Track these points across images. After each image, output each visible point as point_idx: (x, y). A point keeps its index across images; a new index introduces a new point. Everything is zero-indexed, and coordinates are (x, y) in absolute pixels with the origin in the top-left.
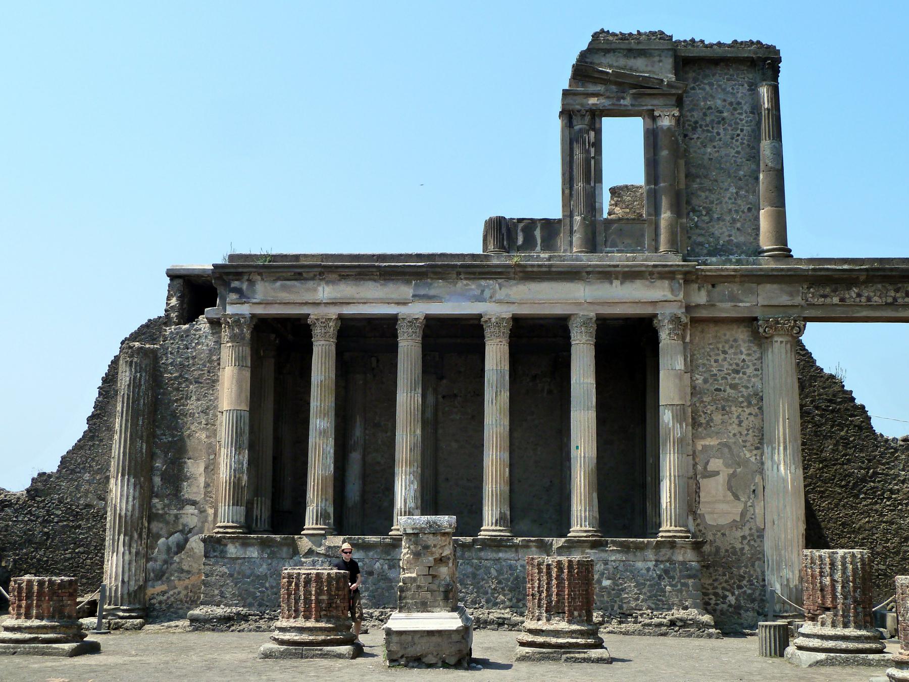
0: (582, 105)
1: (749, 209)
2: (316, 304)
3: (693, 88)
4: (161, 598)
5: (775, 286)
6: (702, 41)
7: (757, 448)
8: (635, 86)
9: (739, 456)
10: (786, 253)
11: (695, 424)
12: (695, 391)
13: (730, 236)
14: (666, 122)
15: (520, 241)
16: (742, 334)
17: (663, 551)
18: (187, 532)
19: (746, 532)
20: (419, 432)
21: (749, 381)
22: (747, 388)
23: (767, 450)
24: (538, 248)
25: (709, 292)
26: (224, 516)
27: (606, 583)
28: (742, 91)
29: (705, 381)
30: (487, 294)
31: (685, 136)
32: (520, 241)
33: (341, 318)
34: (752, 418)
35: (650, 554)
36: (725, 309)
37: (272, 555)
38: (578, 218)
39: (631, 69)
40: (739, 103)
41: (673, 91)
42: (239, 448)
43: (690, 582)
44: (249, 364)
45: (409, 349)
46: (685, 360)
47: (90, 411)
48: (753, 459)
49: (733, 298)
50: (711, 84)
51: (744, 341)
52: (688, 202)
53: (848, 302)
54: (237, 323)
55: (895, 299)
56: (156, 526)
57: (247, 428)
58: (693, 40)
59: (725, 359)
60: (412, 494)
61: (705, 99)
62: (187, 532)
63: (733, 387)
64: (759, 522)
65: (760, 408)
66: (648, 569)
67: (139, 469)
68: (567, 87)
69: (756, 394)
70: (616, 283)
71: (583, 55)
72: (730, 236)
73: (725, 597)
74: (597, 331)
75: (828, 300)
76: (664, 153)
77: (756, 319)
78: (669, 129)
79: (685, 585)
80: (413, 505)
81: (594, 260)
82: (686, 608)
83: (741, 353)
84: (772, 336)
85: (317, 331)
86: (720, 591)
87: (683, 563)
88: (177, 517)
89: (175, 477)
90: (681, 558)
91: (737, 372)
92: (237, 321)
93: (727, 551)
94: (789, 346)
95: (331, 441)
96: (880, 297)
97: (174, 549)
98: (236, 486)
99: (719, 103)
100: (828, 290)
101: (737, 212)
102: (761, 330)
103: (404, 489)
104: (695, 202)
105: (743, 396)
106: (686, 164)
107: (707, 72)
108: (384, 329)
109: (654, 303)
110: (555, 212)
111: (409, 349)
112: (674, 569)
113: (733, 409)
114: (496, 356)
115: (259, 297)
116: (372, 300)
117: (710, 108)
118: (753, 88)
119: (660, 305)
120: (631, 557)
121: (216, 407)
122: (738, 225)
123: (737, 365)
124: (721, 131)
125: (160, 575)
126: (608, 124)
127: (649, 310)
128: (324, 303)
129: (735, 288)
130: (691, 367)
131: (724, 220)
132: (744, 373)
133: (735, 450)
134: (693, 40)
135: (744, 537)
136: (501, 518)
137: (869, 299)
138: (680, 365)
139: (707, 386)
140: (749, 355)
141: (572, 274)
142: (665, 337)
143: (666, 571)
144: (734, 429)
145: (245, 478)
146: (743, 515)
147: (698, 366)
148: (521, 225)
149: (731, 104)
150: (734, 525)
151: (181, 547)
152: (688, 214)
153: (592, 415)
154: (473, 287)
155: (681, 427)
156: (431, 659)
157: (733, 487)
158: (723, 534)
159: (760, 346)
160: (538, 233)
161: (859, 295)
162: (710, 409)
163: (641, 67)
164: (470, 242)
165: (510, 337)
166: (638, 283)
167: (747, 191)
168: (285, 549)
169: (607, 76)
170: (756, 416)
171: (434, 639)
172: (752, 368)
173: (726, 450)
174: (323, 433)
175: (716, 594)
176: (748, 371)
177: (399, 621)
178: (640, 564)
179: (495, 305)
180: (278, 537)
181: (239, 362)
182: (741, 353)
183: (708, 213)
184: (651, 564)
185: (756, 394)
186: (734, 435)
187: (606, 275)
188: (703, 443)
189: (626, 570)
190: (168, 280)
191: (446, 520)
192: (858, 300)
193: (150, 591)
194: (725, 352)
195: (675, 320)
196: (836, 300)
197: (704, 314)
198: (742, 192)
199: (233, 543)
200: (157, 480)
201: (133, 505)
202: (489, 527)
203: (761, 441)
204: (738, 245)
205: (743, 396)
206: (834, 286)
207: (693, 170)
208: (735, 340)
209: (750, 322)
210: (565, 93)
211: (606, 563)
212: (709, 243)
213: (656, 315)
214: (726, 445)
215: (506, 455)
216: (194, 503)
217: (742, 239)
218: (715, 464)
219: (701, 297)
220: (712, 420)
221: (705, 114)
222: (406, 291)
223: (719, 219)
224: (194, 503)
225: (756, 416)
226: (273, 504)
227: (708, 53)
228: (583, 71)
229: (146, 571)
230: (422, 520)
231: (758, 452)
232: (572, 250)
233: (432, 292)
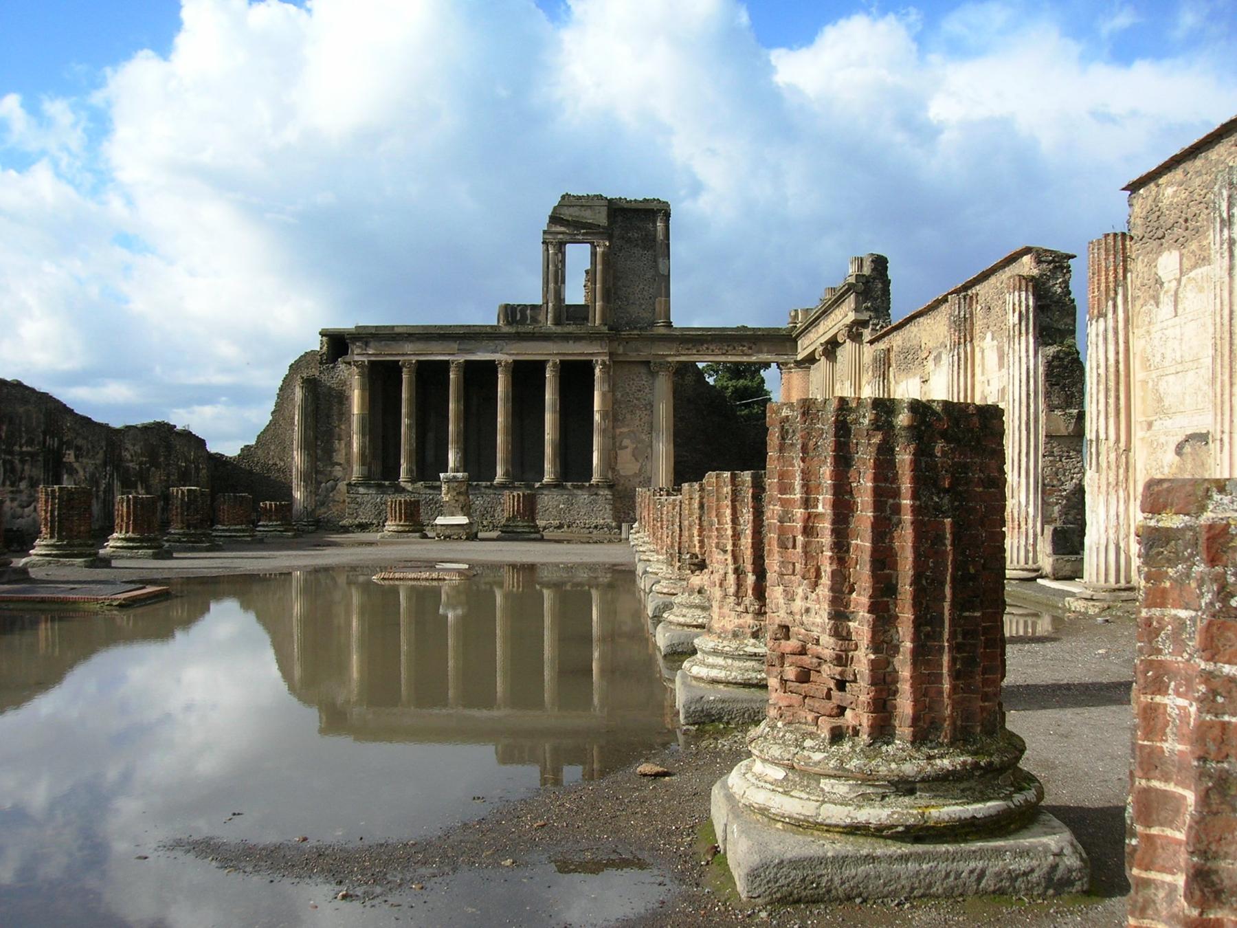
10: (669, 325)
12: (615, 402)
16: (643, 370)
18: (336, 480)
26: (356, 471)
33: (418, 361)
36: (633, 356)
38: (550, 305)
42: (363, 435)
47: (273, 408)
49: (637, 350)
56: (320, 477)
62: (336, 480)
67: (309, 446)
71: (555, 208)
81: (559, 329)
88: (331, 472)
89: (329, 452)
103: (452, 458)
109: (591, 354)
110: (539, 301)
116: (437, 353)
125: (323, 504)
126: (570, 248)
127: (589, 358)
128: (410, 354)
130: (613, 388)
141: (547, 337)
144: (637, 423)
146: (640, 470)
150: (635, 475)
151: (333, 488)
163: (588, 216)
164: (488, 317)
169: (569, 221)
174: (409, 427)
177: (440, 520)
180: (387, 483)
181: (363, 389)
187: (566, 338)
191: (460, 475)
193: (318, 512)
197: (621, 359)
200: (319, 452)
202: (499, 477)
210: (545, 232)
216: (340, 464)
217: (645, 315)
218: (626, 442)
222: (455, 346)
224: (340, 464)
226: (382, 465)
227: (626, 206)
228: (555, 219)
232: (548, 323)
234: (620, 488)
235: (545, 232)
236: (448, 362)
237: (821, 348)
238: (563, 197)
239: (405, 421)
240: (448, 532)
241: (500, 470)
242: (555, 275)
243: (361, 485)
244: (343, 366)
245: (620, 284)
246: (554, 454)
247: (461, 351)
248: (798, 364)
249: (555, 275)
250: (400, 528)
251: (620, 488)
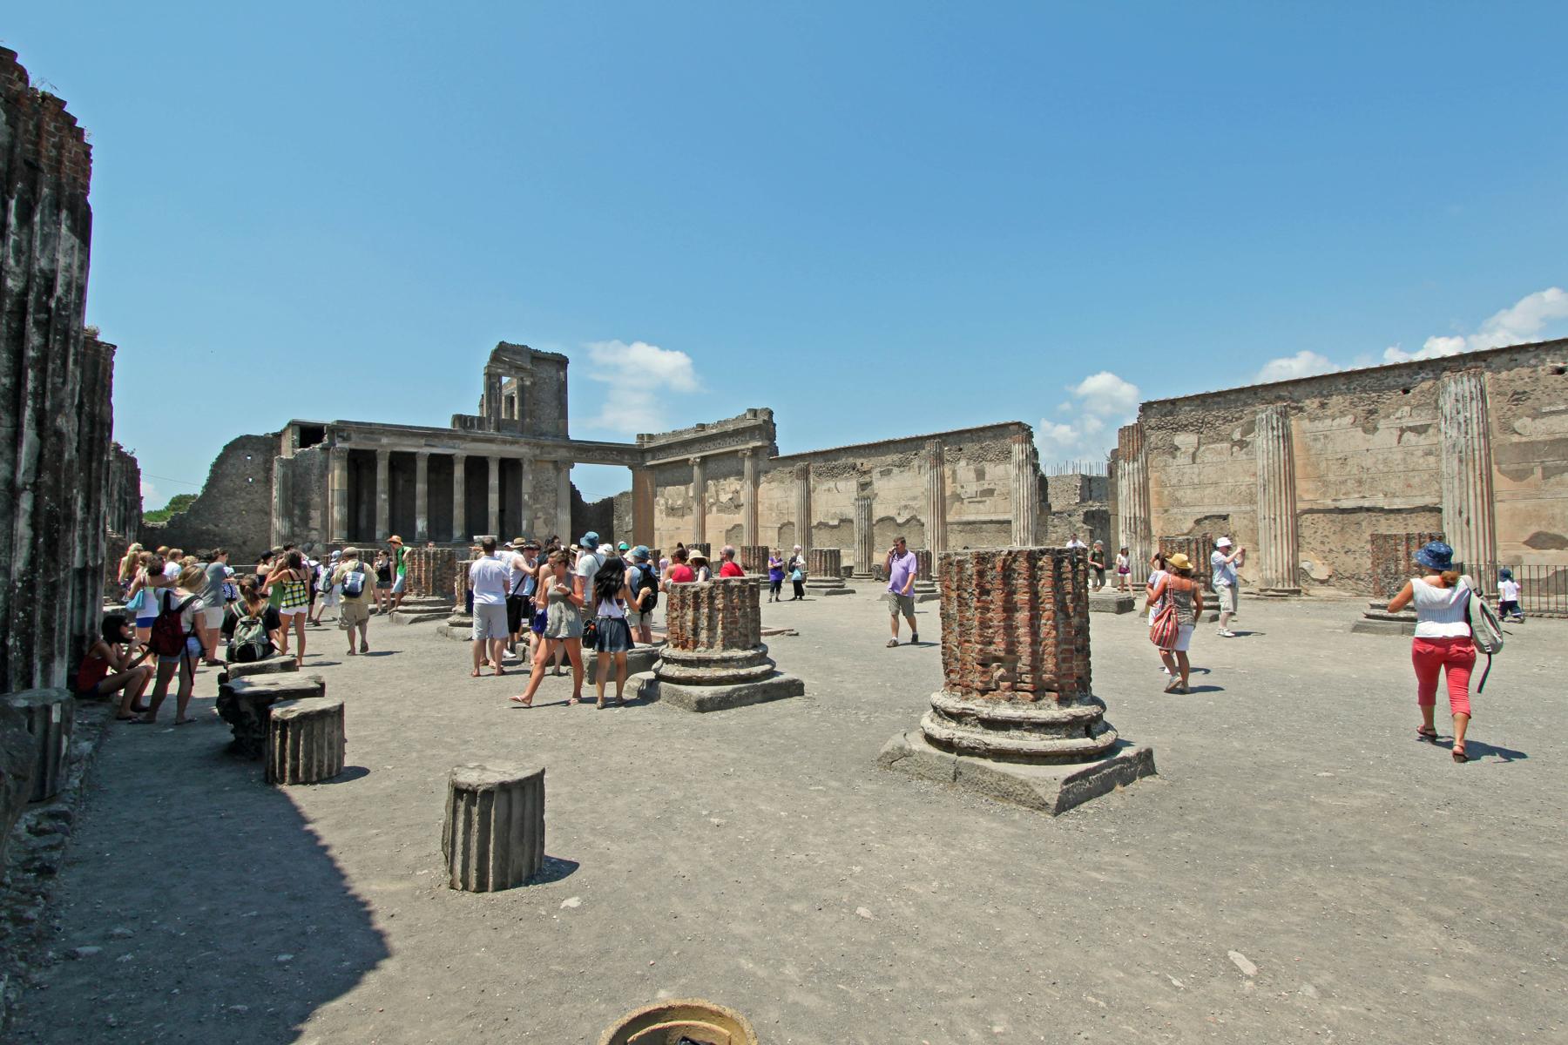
16: (550, 466)
18: (313, 543)
28: (554, 372)
36: (547, 457)
45: (422, 466)
85: (379, 458)
89: (305, 519)
92: (342, 450)
108: (411, 457)
111: (422, 466)
114: (459, 472)
116: (407, 446)
141: (491, 441)
142: (525, 467)
154: (451, 443)
157: (546, 523)
164: (448, 425)
179: (461, 450)
187: (504, 442)
209: (555, 462)
222: (423, 442)
236: (414, 454)
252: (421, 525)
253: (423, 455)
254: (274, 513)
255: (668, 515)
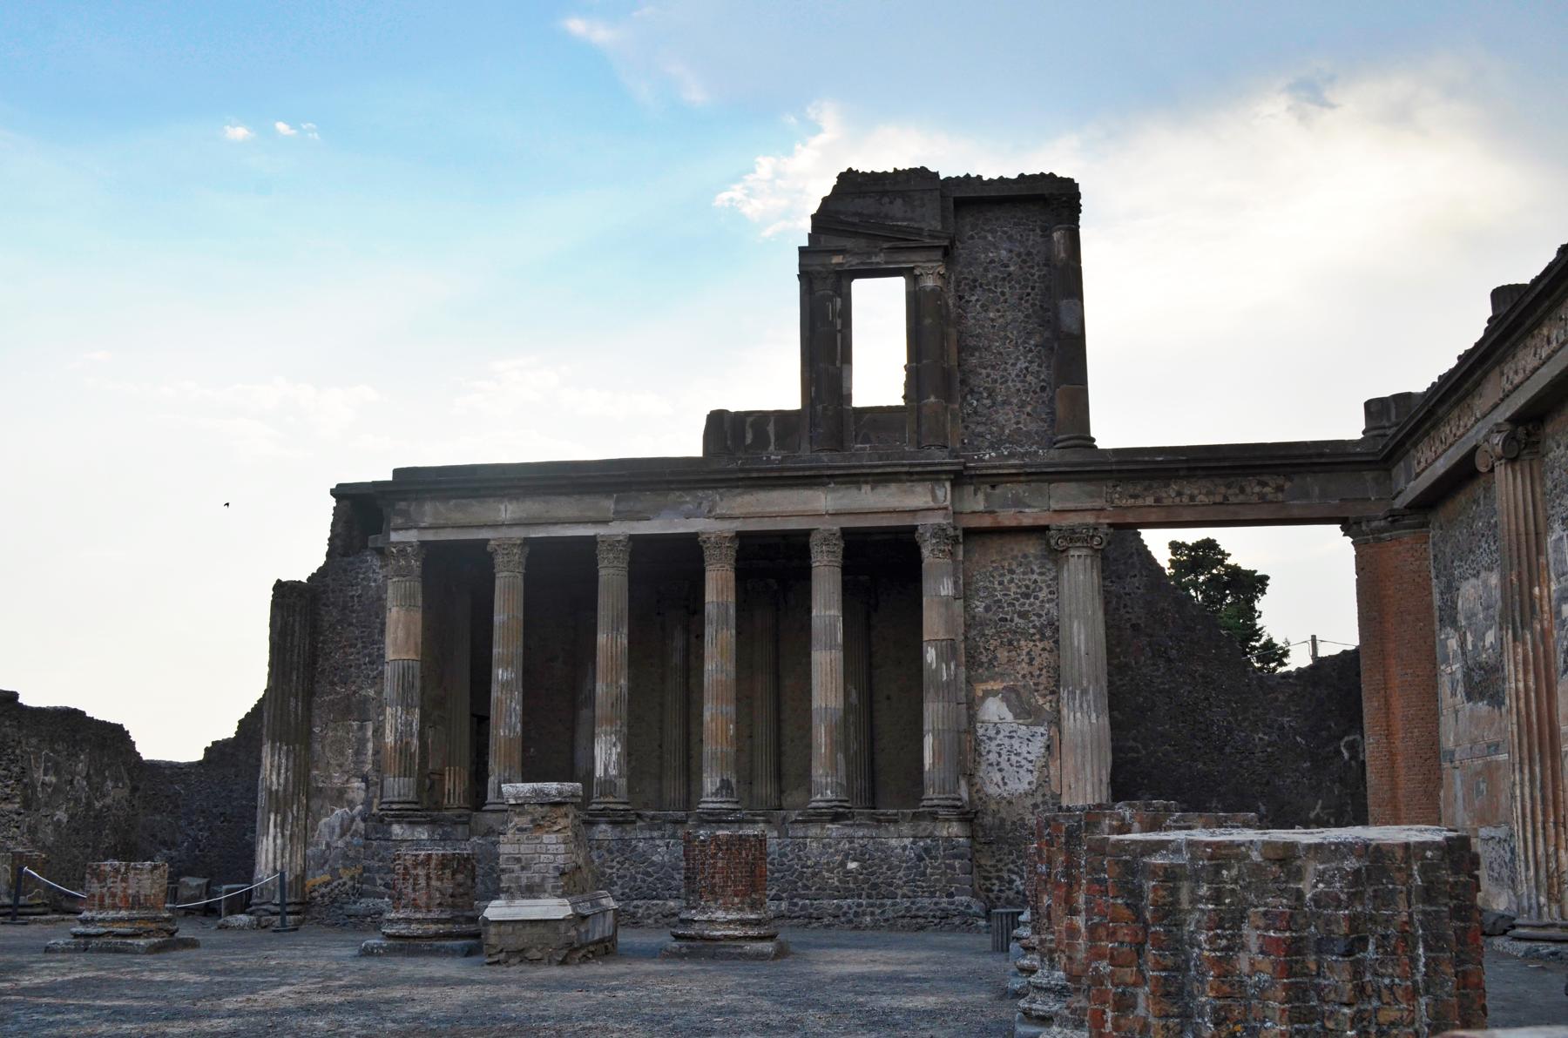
0: (824, 265)
1: (1043, 389)
2: (495, 526)
3: (972, 237)
4: (323, 890)
5: (1073, 485)
6: (979, 177)
7: (1053, 693)
8: (888, 239)
9: (1029, 704)
11: (972, 661)
12: (971, 623)
13: (1018, 423)
14: (929, 283)
15: (749, 441)
16: (1032, 548)
17: (924, 824)
19: (1040, 800)
20: (623, 682)
21: (1042, 607)
22: (1040, 616)
23: (1064, 694)
24: (772, 448)
25: (987, 497)
27: (852, 865)
29: (987, 609)
30: (705, 506)
31: (961, 298)
32: (749, 441)
33: (527, 541)
34: (1045, 655)
35: (905, 828)
36: (1007, 518)
37: (445, 838)
39: (886, 216)
40: (1029, 254)
41: (937, 243)
42: (408, 708)
43: (957, 864)
44: (420, 603)
45: (612, 579)
46: (956, 583)
48: (1047, 707)
49: (1018, 503)
50: (993, 232)
51: (1036, 557)
52: (963, 382)
53: (1167, 502)
54: (402, 552)
55: (1226, 498)
57: (418, 683)
58: (968, 176)
59: (1011, 581)
60: (614, 757)
61: (986, 251)
63: (1023, 615)
64: (1055, 788)
65: (1056, 642)
66: (904, 848)
68: (806, 243)
69: (1051, 624)
70: (866, 488)
72: (1018, 423)
73: (1011, 881)
74: (845, 550)
75: (1140, 502)
76: (928, 321)
77: (1046, 528)
78: (933, 290)
79: (952, 867)
80: (613, 772)
82: (950, 895)
83: (1032, 572)
84: (1067, 549)
85: (499, 560)
86: (1005, 875)
87: (948, 839)
90: (945, 833)
91: (1027, 596)
93: (1014, 823)
94: (1088, 561)
95: (518, 695)
96: (1207, 494)
97: (338, 830)
98: (403, 749)
99: (1003, 252)
100: (1139, 489)
101: (1026, 392)
102: (1053, 542)
104: (973, 381)
105: (1034, 627)
106: (960, 333)
107: (989, 215)
109: (914, 512)
110: (790, 399)
111: (612, 579)
112: (937, 847)
113: (1022, 643)
114: (719, 587)
115: (427, 521)
117: (992, 261)
118: (1046, 233)
119: (920, 514)
120: (883, 832)
121: (383, 656)
122: (1029, 409)
123: (1027, 587)
124: (1007, 290)
127: (907, 521)
128: (505, 524)
129: (1020, 489)
130: (965, 592)
131: (1010, 404)
132: (1036, 598)
133: (1025, 694)
134: (968, 176)
135: (1035, 806)
136: (722, 787)
137: (1192, 498)
138: (947, 589)
139: (989, 615)
140: (1041, 574)
142: (926, 552)
143: (927, 850)
144: (1024, 668)
145: (415, 741)
147: (977, 590)
148: (750, 420)
149: (1019, 255)
152: (964, 398)
153: (838, 655)
155: (948, 668)
156: (534, 954)
158: (1010, 803)
159: (1056, 562)
160: (771, 429)
161: (1179, 494)
162: (993, 643)
165: (737, 560)
166: (893, 487)
167: (1040, 366)
168: (460, 828)
170: (1051, 651)
171: (540, 930)
172: (1046, 590)
173: (1013, 696)
174: (505, 685)
175: (1000, 878)
176: (1041, 595)
178: (893, 842)
179: (714, 521)
181: (406, 601)
182: (1032, 572)
183: (990, 395)
184: (907, 841)
185: (1051, 624)
186: (1024, 676)
187: (853, 478)
188: (984, 687)
189: (877, 850)
190: (333, 502)
192: (1177, 500)
193: (310, 882)
194: (1012, 572)
195: (939, 532)
196: (1150, 501)
198: (1034, 367)
199: (399, 822)
201: (287, 779)
203: (1058, 686)
204: (1028, 434)
205: (1034, 627)
206: (1147, 483)
207: (972, 342)
208: (1025, 556)
210: (802, 250)
211: (851, 840)
212: (991, 433)
213: (916, 527)
214: (1012, 689)
215: (731, 709)
219: (979, 504)
220: (995, 658)
221: (986, 270)
222: (608, 505)
223: (1004, 403)
225: (1051, 651)
228: (825, 220)
229: (305, 857)
230: (526, 788)
231: (1054, 698)
233: (639, 506)
234: (988, 820)
235: (802, 250)
236: (592, 541)
237: (1497, 439)
238: (841, 177)
239: (500, 674)
240: (512, 942)
241: (710, 783)
242: (826, 343)
243: (399, 818)
244: (377, 563)
245: (974, 361)
246: (833, 745)
247: (621, 516)
248: (1395, 518)
249: (826, 343)
250: (415, 929)
251: (988, 820)
252: (606, 755)
253: (613, 543)
254: (265, 731)
255: (1469, 698)
